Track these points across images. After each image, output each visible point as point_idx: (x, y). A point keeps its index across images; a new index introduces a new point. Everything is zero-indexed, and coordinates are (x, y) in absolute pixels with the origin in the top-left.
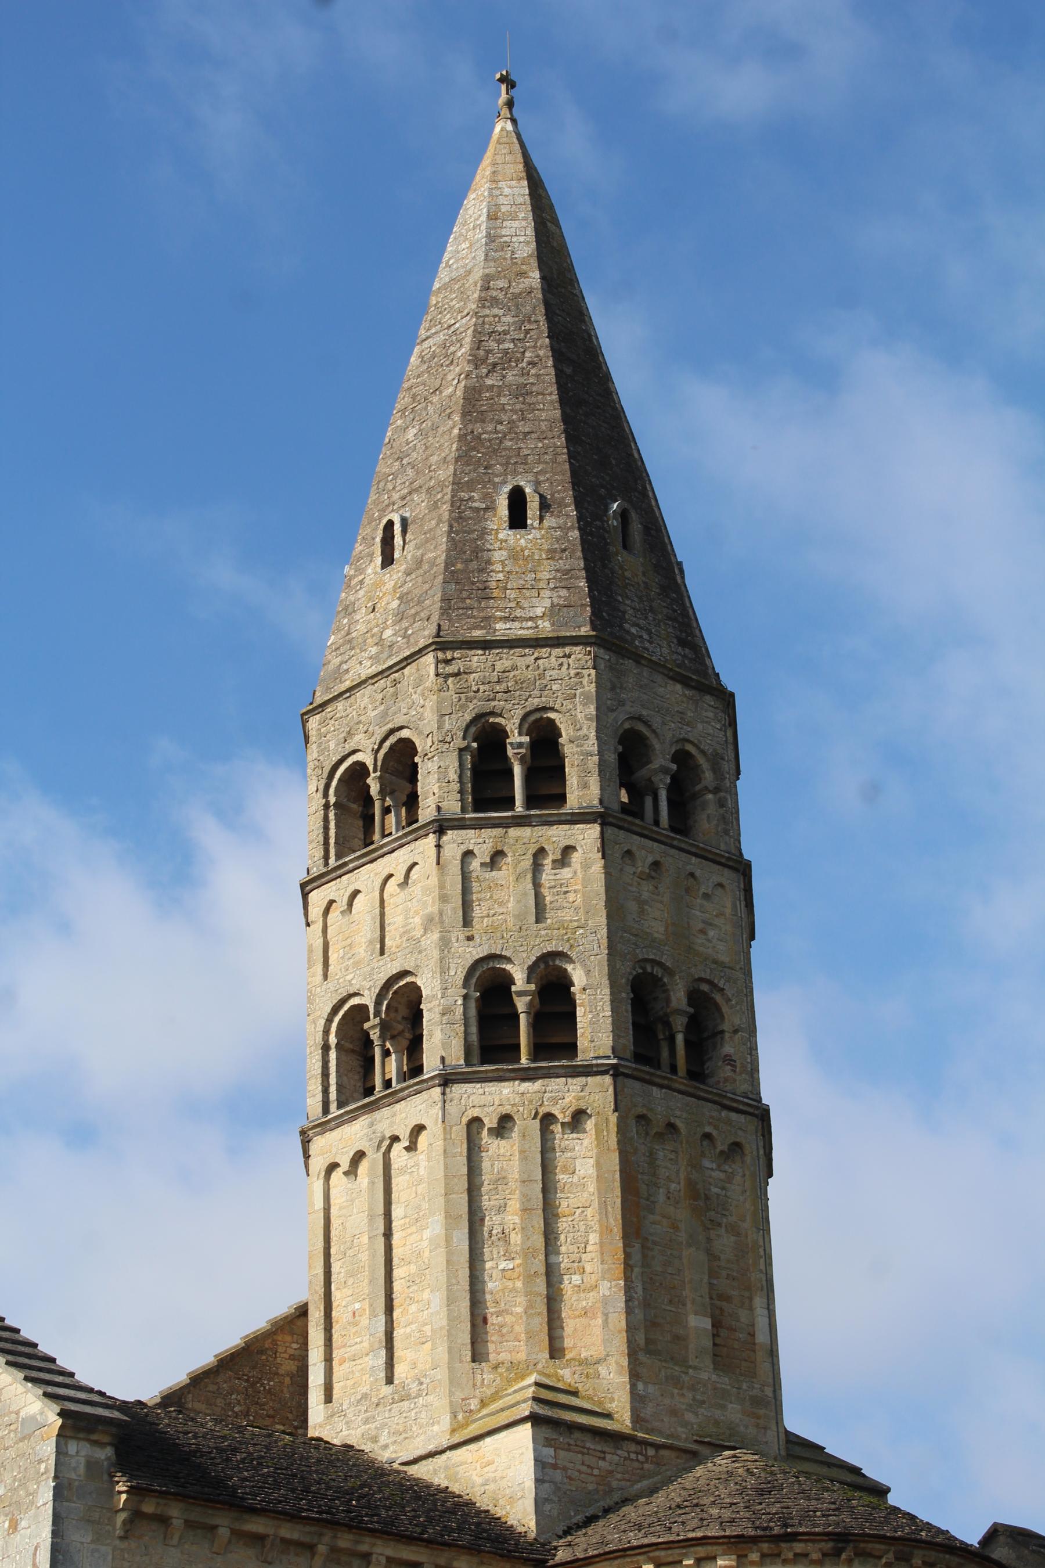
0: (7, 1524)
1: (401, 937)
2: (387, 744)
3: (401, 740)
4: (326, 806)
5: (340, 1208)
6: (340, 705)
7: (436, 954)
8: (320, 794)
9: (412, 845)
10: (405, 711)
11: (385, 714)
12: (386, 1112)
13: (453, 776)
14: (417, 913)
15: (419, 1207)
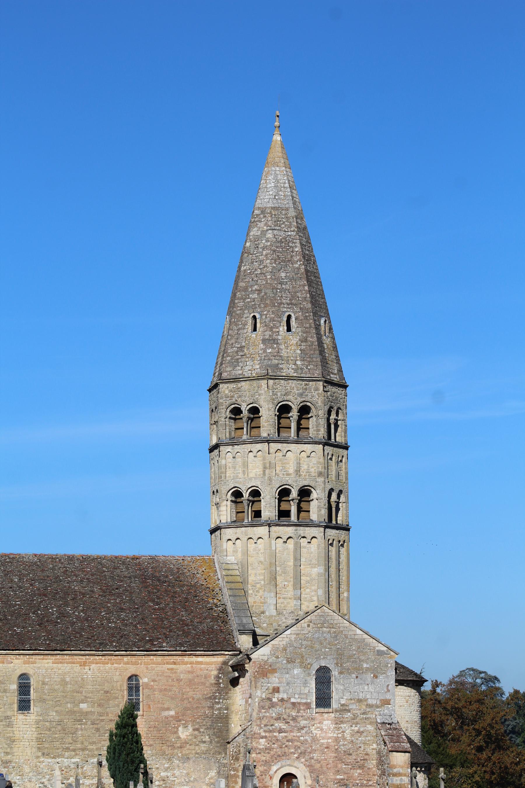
0: (372, 675)
1: (306, 472)
2: (301, 404)
3: (306, 405)
4: (276, 415)
5: (279, 551)
6: (282, 381)
7: (323, 485)
8: (273, 409)
9: (314, 445)
10: (311, 397)
11: (301, 395)
12: (302, 528)
13: (326, 427)
14: (312, 467)
15: (311, 561)
